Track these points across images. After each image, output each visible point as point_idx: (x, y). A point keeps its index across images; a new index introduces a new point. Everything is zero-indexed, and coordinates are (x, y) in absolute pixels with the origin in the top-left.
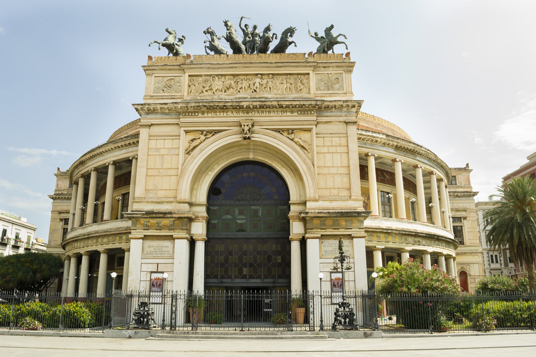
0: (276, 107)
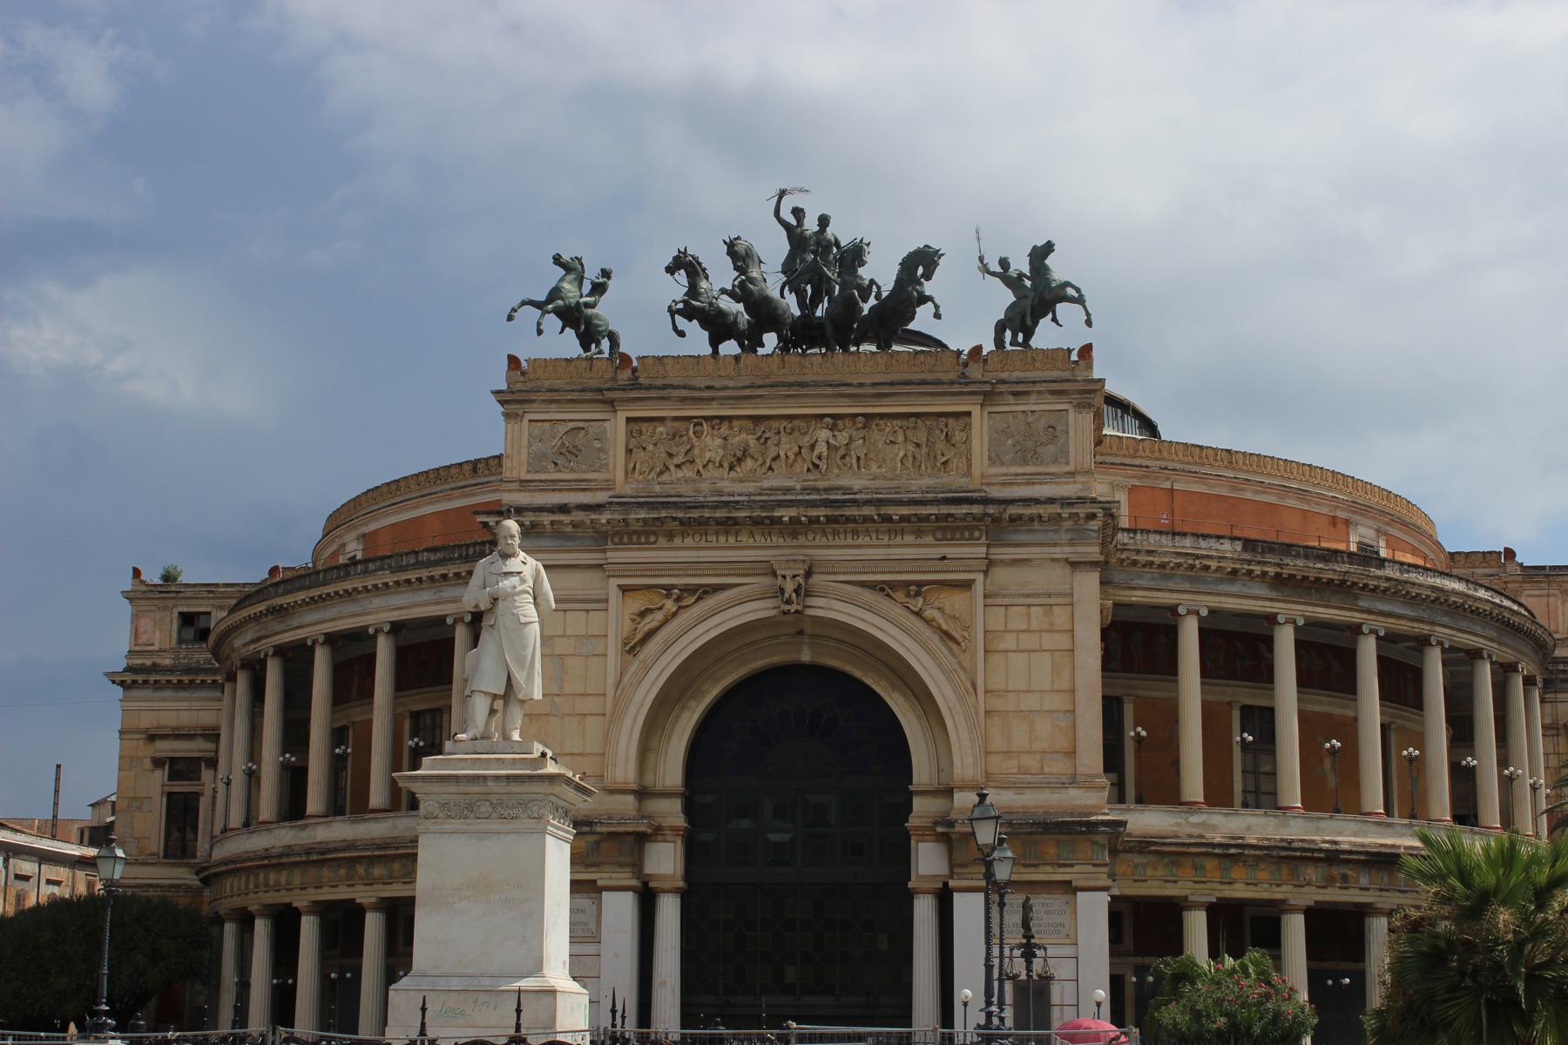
0: (874, 521)
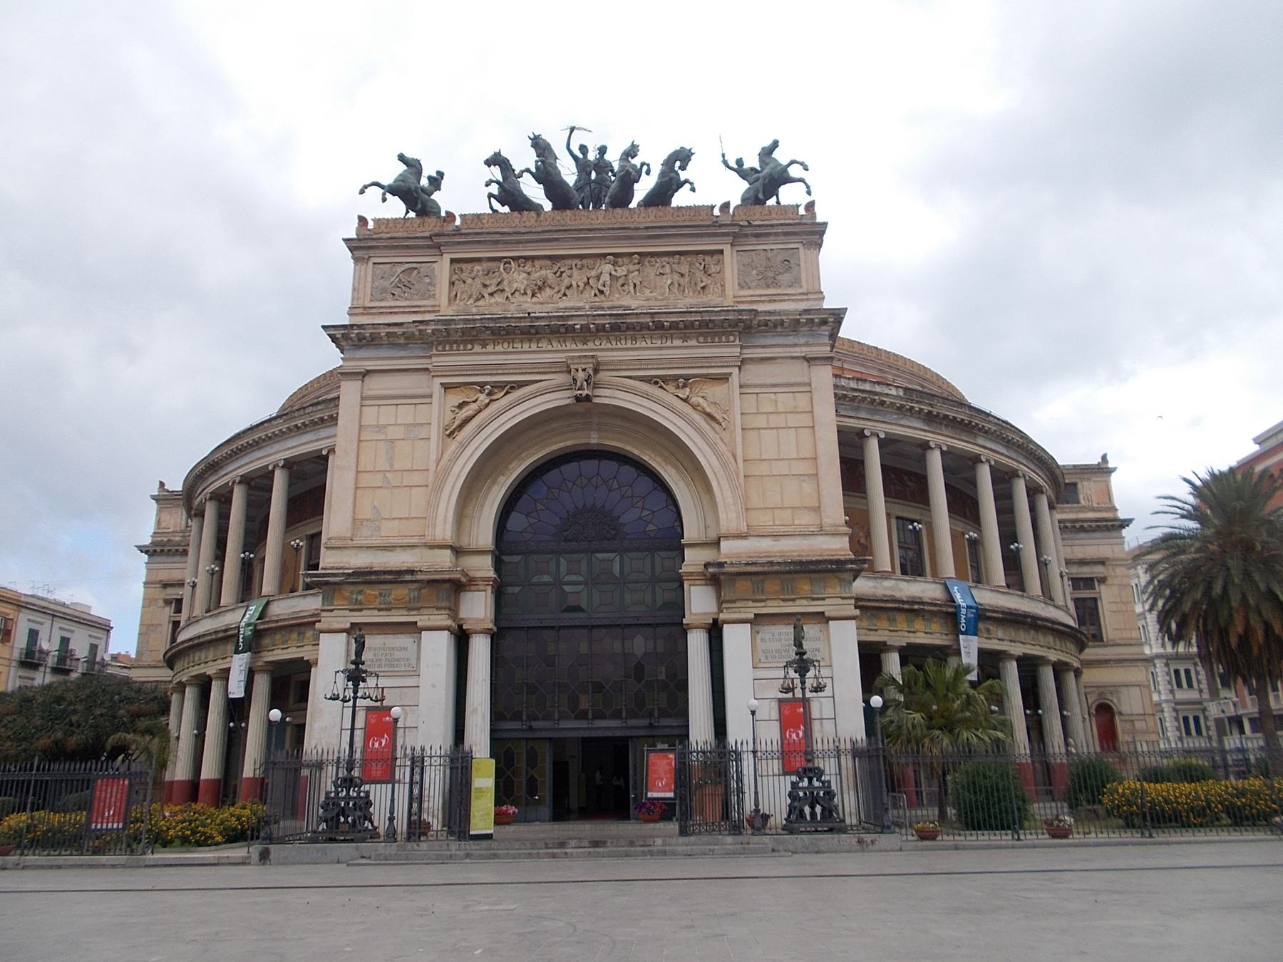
0: (649, 328)
